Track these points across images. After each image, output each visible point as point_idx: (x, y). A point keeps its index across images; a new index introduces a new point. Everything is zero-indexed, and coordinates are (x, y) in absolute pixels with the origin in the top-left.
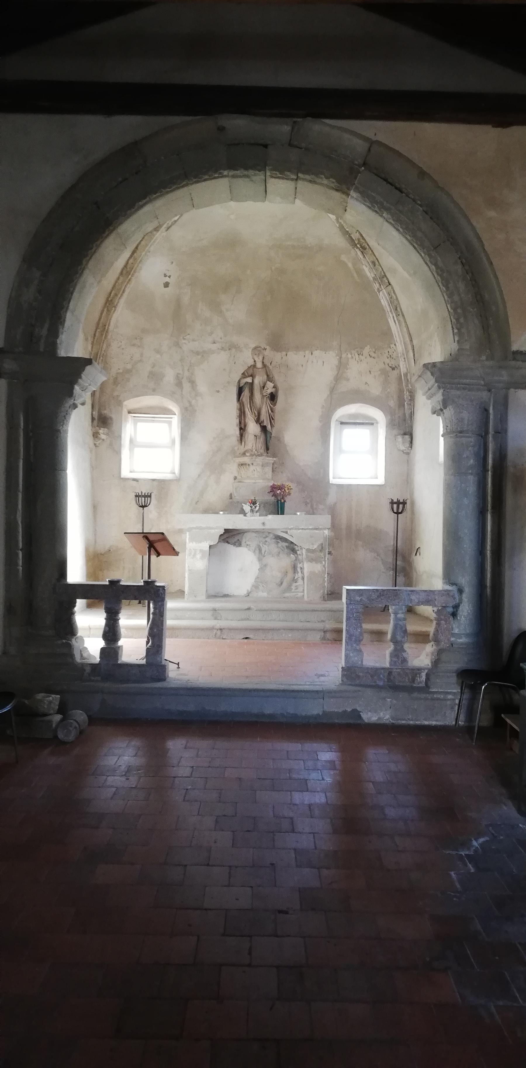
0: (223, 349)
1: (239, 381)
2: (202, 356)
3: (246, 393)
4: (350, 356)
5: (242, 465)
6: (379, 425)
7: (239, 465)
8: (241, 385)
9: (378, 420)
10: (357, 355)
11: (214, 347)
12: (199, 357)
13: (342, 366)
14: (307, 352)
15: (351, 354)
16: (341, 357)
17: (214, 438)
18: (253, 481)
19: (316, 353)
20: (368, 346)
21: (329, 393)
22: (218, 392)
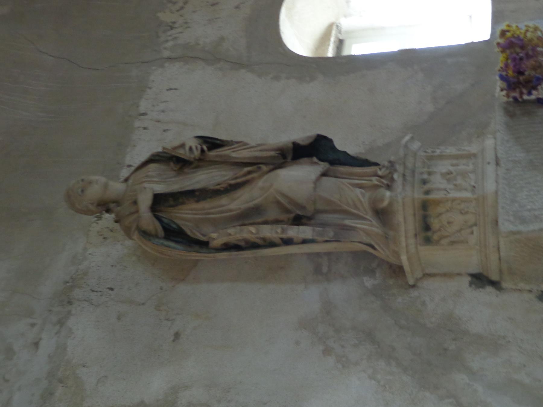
0: (61, 323)
1: (145, 234)
2: (61, 381)
3: (185, 216)
4: (170, 44)
5: (427, 228)
6: (346, 24)
7: (428, 241)
8: (161, 233)
9: (332, 20)
10: (173, 32)
11: (48, 344)
12: (59, 391)
13: (189, 55)
14: (137, 124)
15: (167, 41)
16: (170, 59)
17: (327, 351)
18: (490, 169)
19: (144, 106)
20: (159, 15)
21: (243, 71)
22: (177, 335)
